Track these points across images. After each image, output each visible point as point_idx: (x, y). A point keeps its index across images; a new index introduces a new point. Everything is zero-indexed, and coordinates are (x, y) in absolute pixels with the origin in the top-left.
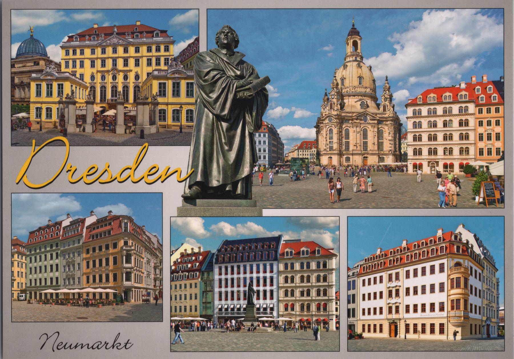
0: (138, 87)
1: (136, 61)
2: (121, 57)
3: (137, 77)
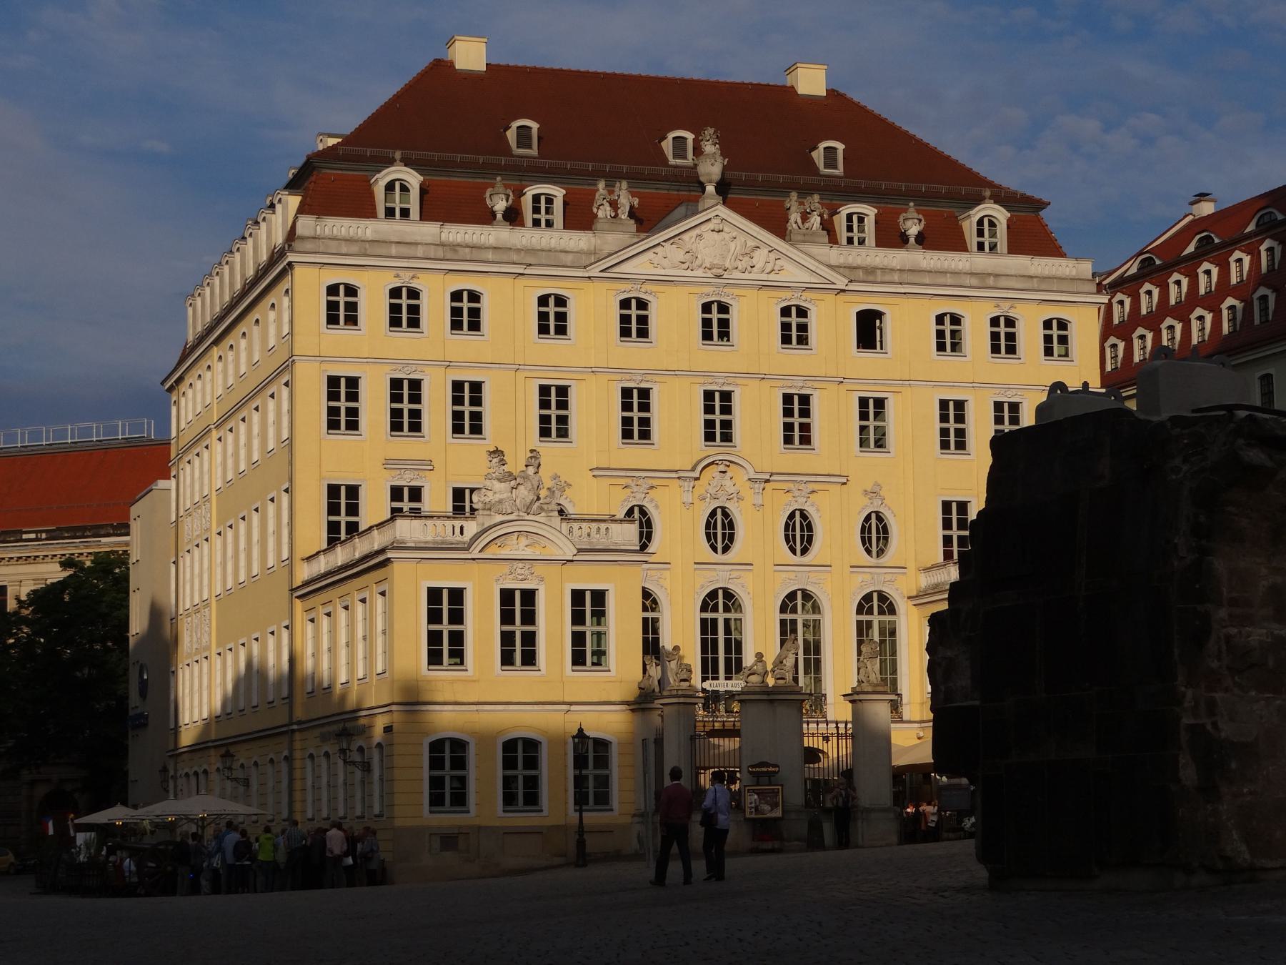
3: (875, 533)
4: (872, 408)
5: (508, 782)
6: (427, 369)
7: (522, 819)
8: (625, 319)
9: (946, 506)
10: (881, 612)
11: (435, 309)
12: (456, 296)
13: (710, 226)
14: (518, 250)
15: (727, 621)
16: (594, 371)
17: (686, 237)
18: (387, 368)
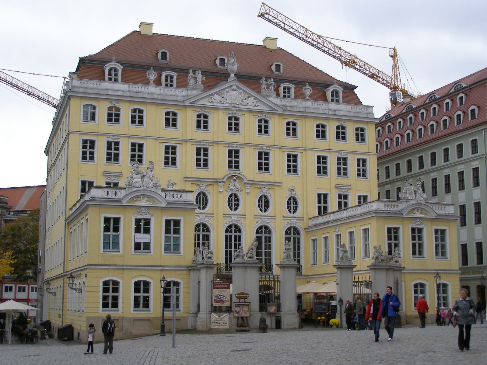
0: (296, 231)
2: (251, 145)
3: (292, 204)
4: (292, 159)
5: (136, 298)
7: (142, 314)
8: (199, 122)
9: (319, 195)
10: (294, 234)
11: (126, 114)
12: (134, 111)
13: (233, 88)
14: (158, 95)
15: (236, 237)
16: (186, 141)
17: (222, 92)
18: (105, 137)
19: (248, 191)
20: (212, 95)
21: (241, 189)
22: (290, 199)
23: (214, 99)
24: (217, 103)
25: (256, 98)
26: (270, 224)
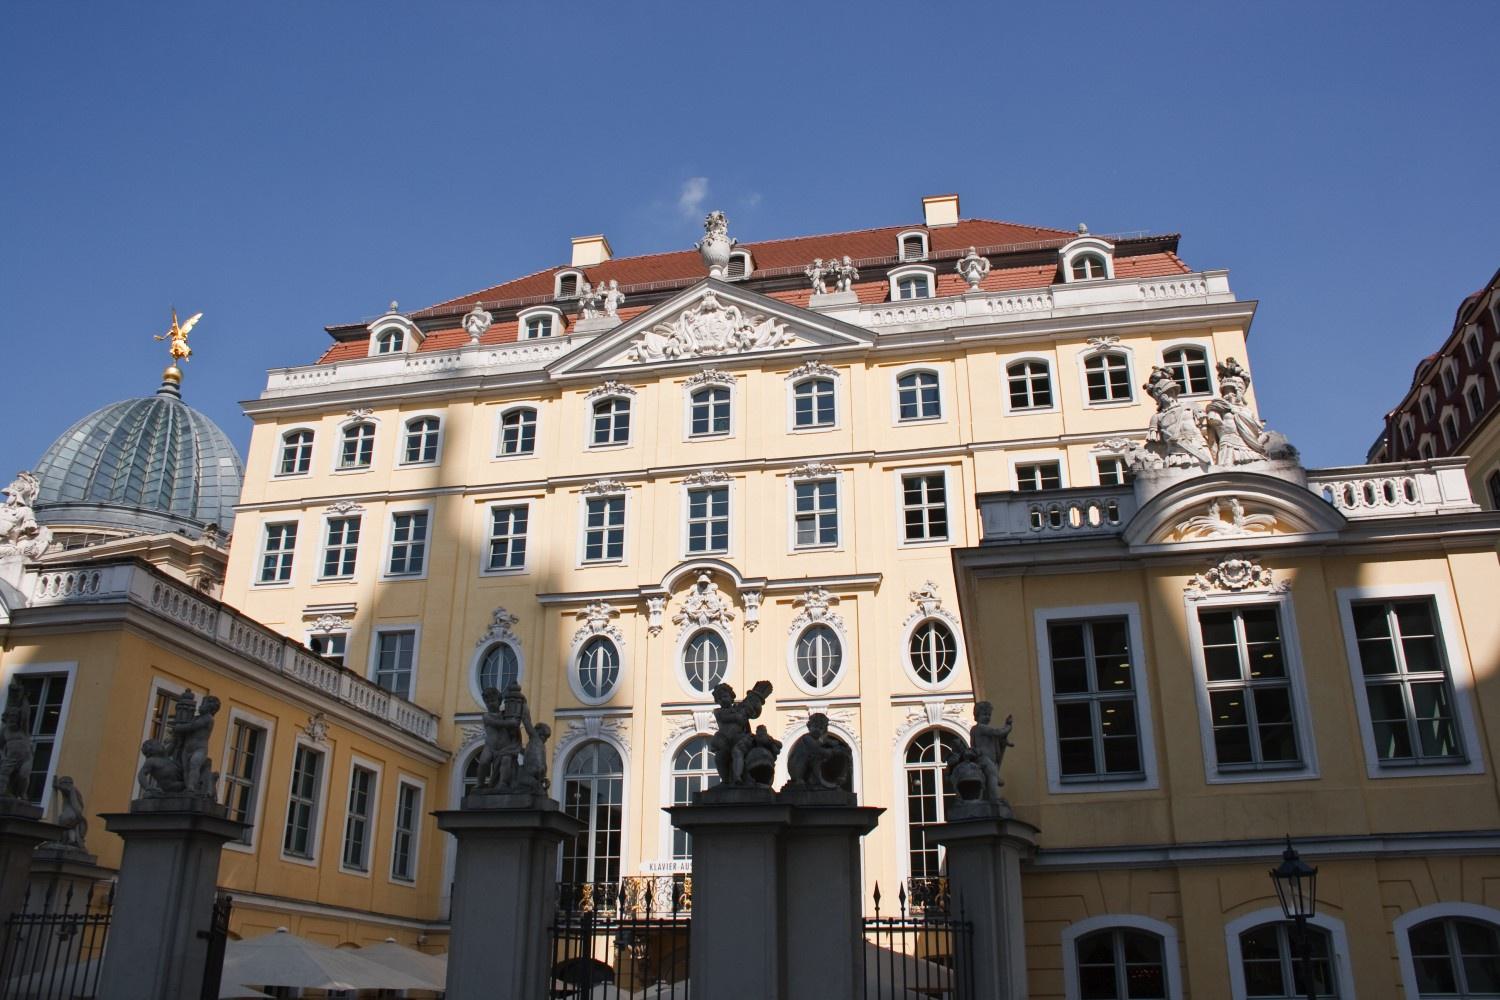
1: (912, 498)
6: (365, 505)
18: (324, 509)
19: (751, 615)
20: (639, 336)
21: (729, 612)
22: (922, 629)
23: (645, 348)
24: (651, 356)
25: (781, 318)
26: (839, 725)
